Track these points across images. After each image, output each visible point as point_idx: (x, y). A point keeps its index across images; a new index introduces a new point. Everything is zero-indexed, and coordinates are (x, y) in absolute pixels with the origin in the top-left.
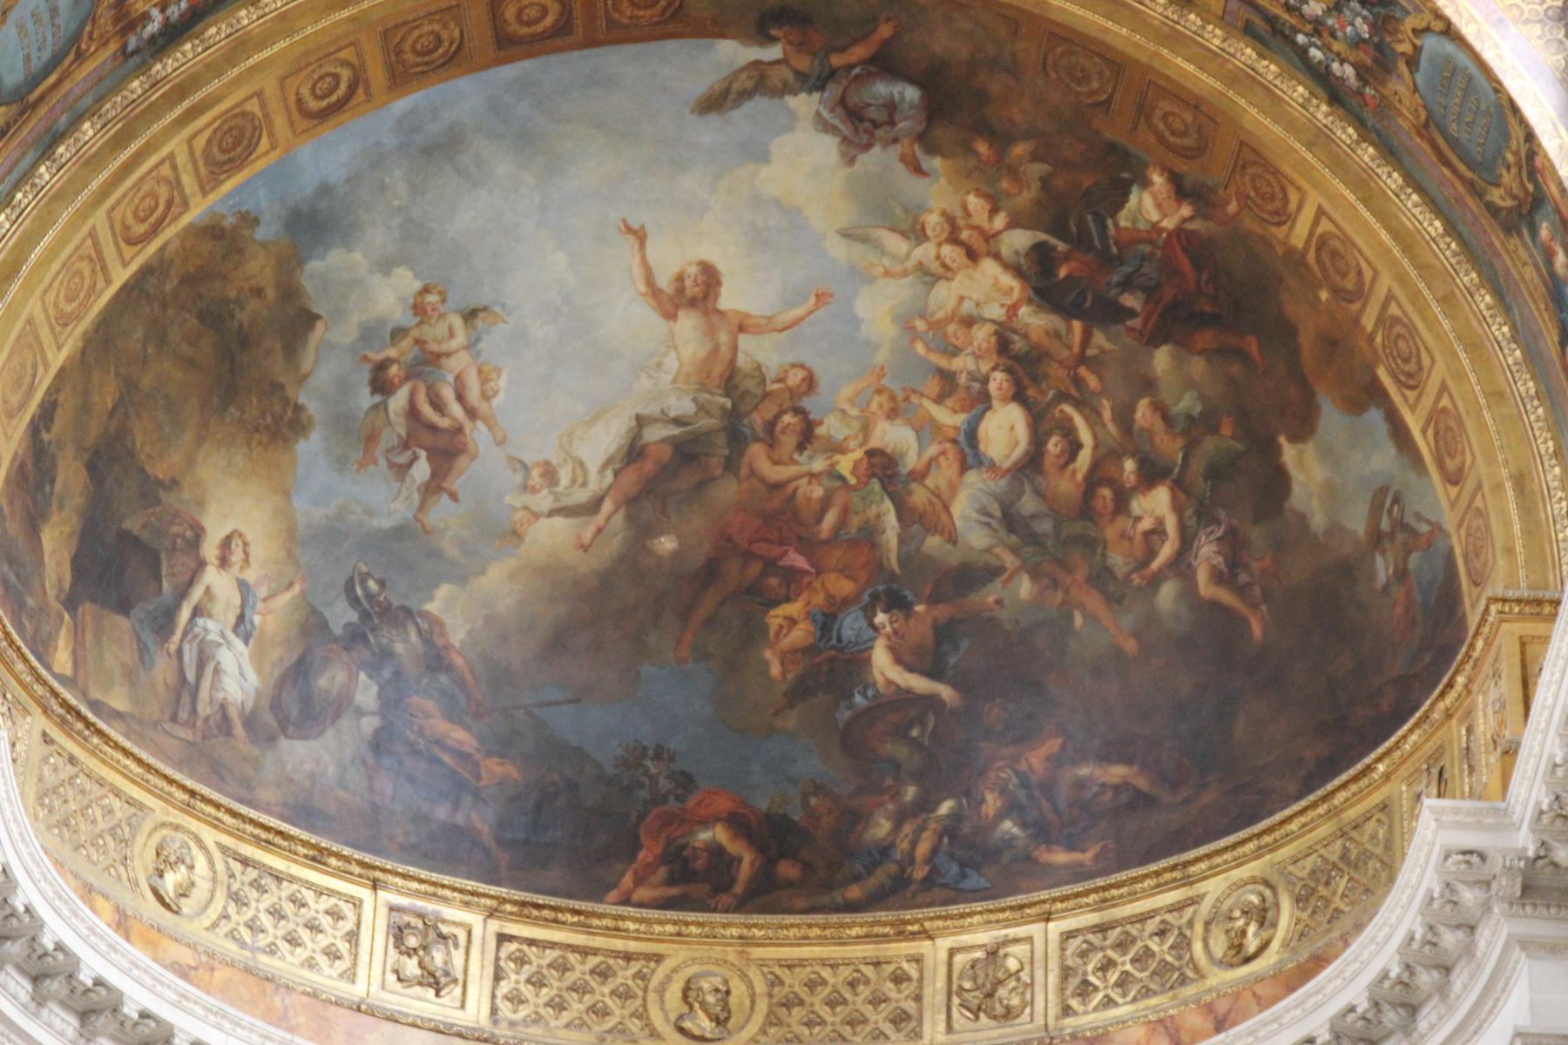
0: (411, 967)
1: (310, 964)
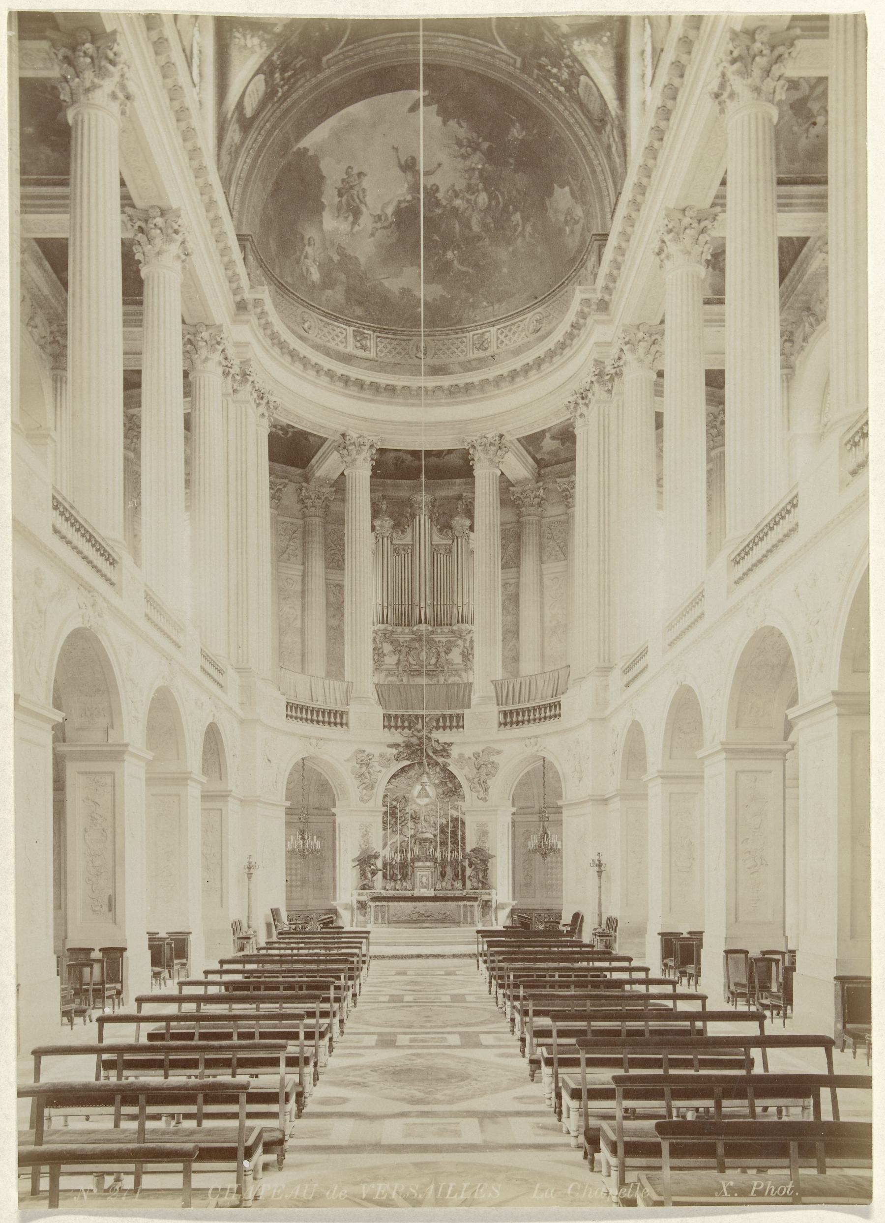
0: (359, 345)
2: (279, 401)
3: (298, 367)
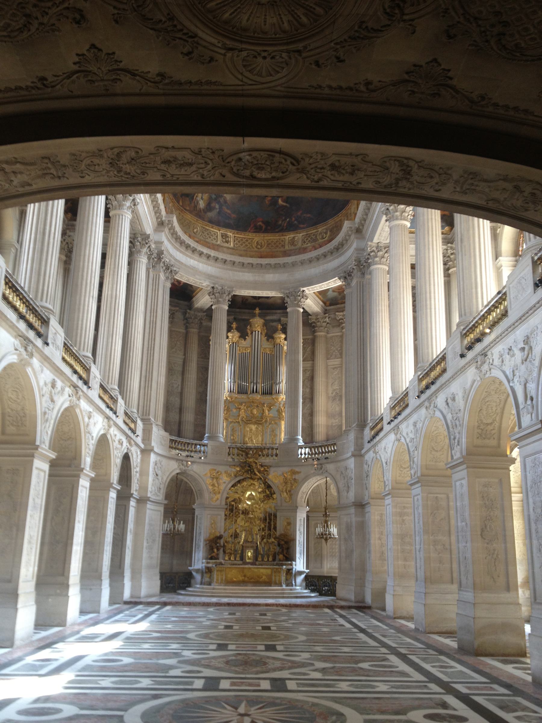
0: (224, 240)
1: (212, 240)
2: (177, 270)
3: (189, 253)
